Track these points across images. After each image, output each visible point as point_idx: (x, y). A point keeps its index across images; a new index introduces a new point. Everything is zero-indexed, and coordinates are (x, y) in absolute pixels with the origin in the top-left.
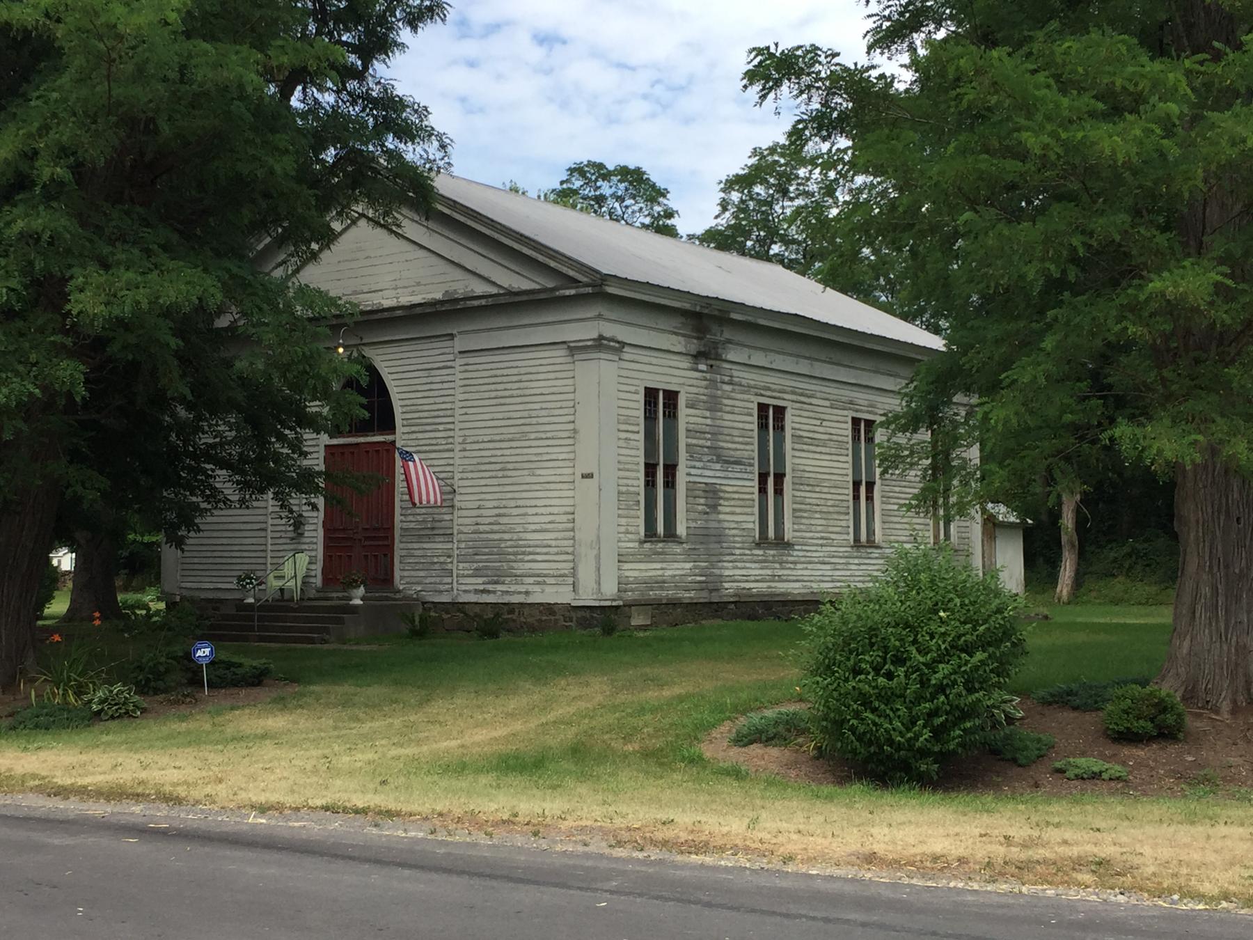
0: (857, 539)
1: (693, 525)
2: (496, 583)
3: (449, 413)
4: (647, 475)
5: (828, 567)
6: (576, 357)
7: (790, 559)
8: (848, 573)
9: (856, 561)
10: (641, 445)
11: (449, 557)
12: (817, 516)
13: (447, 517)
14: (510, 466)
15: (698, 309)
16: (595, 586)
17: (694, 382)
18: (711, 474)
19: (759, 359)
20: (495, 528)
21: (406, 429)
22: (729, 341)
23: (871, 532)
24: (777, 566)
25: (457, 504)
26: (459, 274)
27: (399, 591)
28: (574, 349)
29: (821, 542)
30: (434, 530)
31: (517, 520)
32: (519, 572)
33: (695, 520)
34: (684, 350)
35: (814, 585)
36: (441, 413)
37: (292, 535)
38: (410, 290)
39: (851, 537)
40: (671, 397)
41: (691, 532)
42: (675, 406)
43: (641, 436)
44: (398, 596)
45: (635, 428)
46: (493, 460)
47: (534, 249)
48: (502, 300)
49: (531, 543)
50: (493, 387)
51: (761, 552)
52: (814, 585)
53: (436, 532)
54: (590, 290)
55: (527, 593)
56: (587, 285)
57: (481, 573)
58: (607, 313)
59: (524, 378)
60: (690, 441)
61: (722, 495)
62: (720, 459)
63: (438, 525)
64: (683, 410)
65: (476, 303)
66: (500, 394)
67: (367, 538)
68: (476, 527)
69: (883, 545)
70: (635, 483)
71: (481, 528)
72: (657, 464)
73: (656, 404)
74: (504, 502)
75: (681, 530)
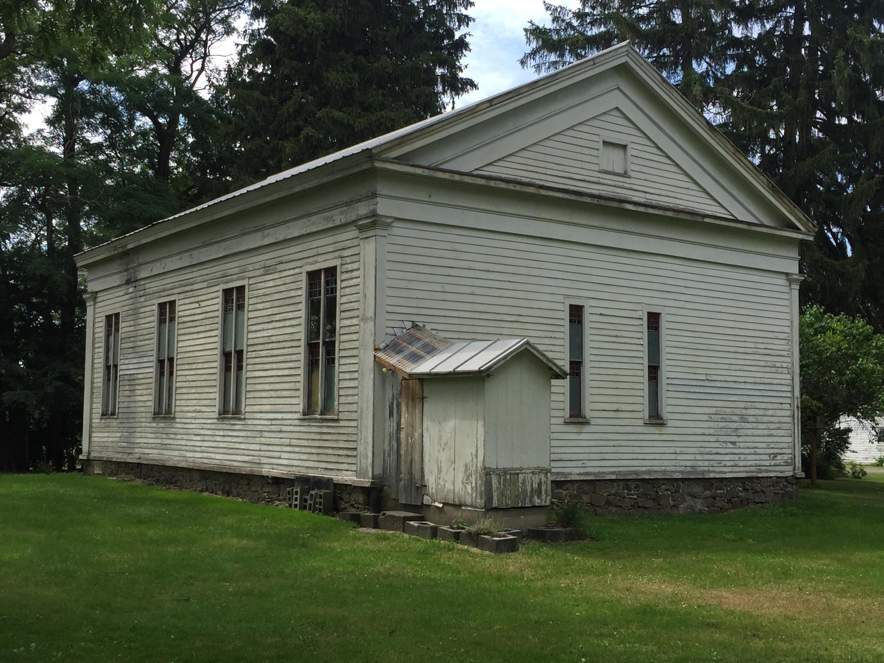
5: (198, 438)
7: (173, 430)
9: (221, 433)
19: (158, 269)
24: (164, 436)
35: (189, 454)
51: (154, 425)
52: (189, 454)
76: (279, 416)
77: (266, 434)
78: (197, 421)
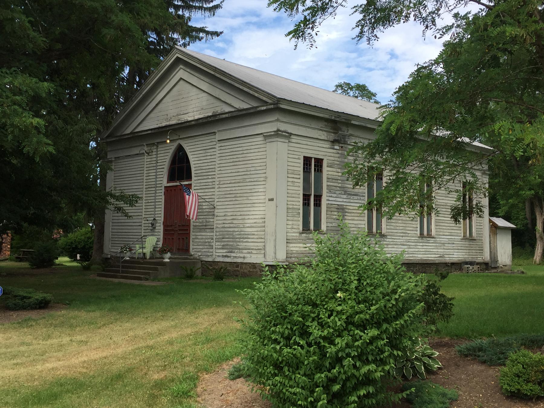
0: (422, 234)
1: (330, 225)
2: (231, 252)
3: (213, 170)
4: (304, 199)
5: (406, 247)
6: (267, 141)
7: (384, 242)
8: (417, 250)
9: (421, 244)
10: (301, 185)
11: (212, 239)
12: (400, 222)
13: (212, 220)
14: (238, 195)
15: (333, 118)
16: (274, 255)
17: (332, 155)
18: (342, 200)
20: (232, 225)
21: (196, 178)
22: (351, 135)
23: (429, 230)
25: (216, 214)
26: (218, 103)
27: (192, 255)
28: (267, 137)
29: (402, 235)
30: (206, 227)
31: (241, 222)
32: (241, 247)
33: (331, 223)
34: (326, 139)
36: (210, 170)
37: (151, 228)
38: (199, 112)
39: (418, 232)
40: (319, 162)
41: (329, 228)
42: (321, 166)
43: (301, 181)
44: (192, 258)
45: (298, 177)
46: (231, 192)
47: (249, 88)
48: (235, 114)
49: (246, 233)
50: (231, 157)
53: (207, 227)
54: (272, 106)
55: (244, 258)
56: (271, 104)
57: (224, 247)
58: (281, 118)
59: (245, 152)
60: (329, 183)
61: (347, 210)
62: (346, 193)
63: (208, 224)
64: (325, 168)
65: (224, 116)
66: (234, 160)
67: (180, 230)
68: (223, 225)
69: (436, 236)
70: (297, 203)
71: (226, 225)
72: (310, 195)
73: (310, 165)
74: (235, 213)
75: (324, 227)
76: (453, 237)
77: (446, 245)
78: (404, 238)
